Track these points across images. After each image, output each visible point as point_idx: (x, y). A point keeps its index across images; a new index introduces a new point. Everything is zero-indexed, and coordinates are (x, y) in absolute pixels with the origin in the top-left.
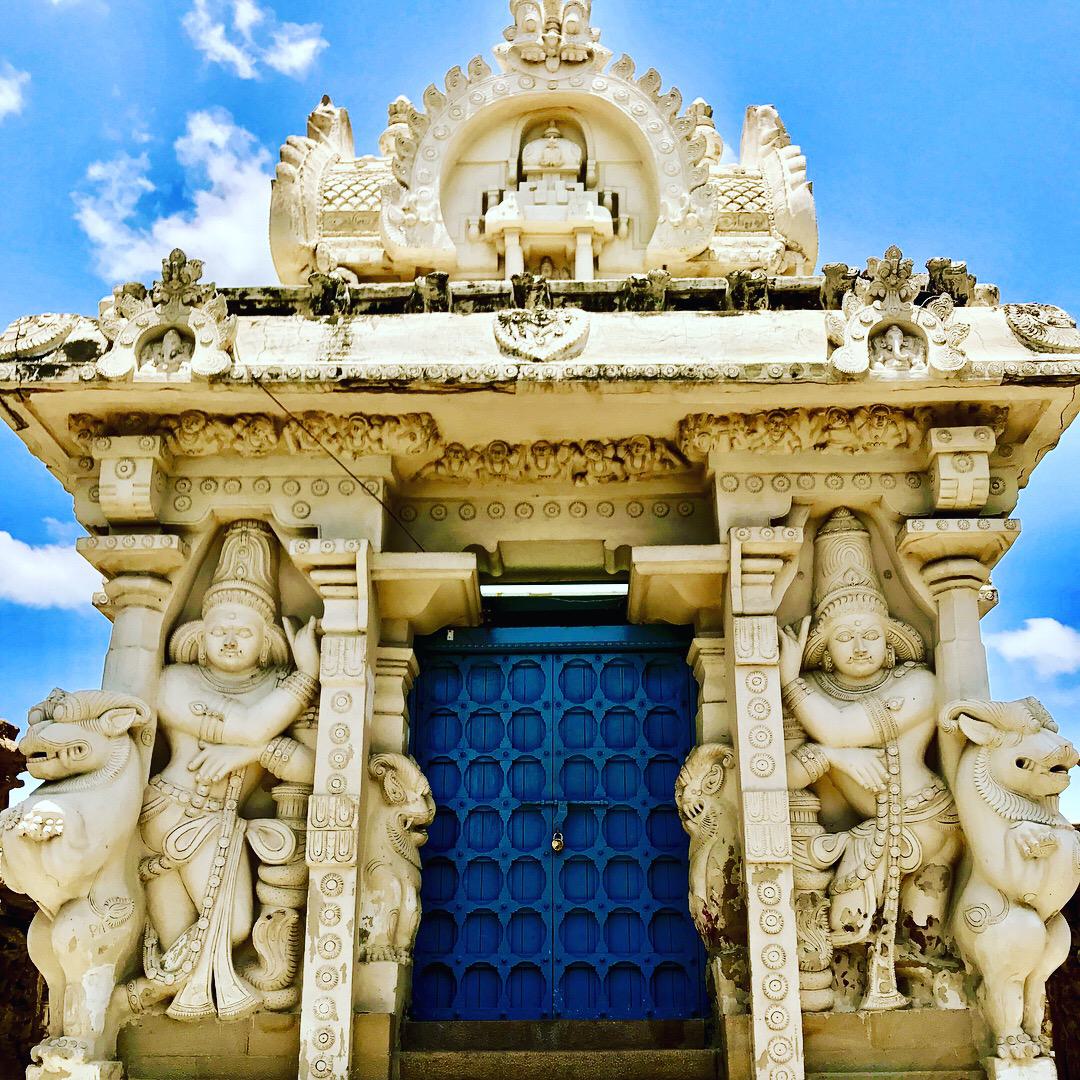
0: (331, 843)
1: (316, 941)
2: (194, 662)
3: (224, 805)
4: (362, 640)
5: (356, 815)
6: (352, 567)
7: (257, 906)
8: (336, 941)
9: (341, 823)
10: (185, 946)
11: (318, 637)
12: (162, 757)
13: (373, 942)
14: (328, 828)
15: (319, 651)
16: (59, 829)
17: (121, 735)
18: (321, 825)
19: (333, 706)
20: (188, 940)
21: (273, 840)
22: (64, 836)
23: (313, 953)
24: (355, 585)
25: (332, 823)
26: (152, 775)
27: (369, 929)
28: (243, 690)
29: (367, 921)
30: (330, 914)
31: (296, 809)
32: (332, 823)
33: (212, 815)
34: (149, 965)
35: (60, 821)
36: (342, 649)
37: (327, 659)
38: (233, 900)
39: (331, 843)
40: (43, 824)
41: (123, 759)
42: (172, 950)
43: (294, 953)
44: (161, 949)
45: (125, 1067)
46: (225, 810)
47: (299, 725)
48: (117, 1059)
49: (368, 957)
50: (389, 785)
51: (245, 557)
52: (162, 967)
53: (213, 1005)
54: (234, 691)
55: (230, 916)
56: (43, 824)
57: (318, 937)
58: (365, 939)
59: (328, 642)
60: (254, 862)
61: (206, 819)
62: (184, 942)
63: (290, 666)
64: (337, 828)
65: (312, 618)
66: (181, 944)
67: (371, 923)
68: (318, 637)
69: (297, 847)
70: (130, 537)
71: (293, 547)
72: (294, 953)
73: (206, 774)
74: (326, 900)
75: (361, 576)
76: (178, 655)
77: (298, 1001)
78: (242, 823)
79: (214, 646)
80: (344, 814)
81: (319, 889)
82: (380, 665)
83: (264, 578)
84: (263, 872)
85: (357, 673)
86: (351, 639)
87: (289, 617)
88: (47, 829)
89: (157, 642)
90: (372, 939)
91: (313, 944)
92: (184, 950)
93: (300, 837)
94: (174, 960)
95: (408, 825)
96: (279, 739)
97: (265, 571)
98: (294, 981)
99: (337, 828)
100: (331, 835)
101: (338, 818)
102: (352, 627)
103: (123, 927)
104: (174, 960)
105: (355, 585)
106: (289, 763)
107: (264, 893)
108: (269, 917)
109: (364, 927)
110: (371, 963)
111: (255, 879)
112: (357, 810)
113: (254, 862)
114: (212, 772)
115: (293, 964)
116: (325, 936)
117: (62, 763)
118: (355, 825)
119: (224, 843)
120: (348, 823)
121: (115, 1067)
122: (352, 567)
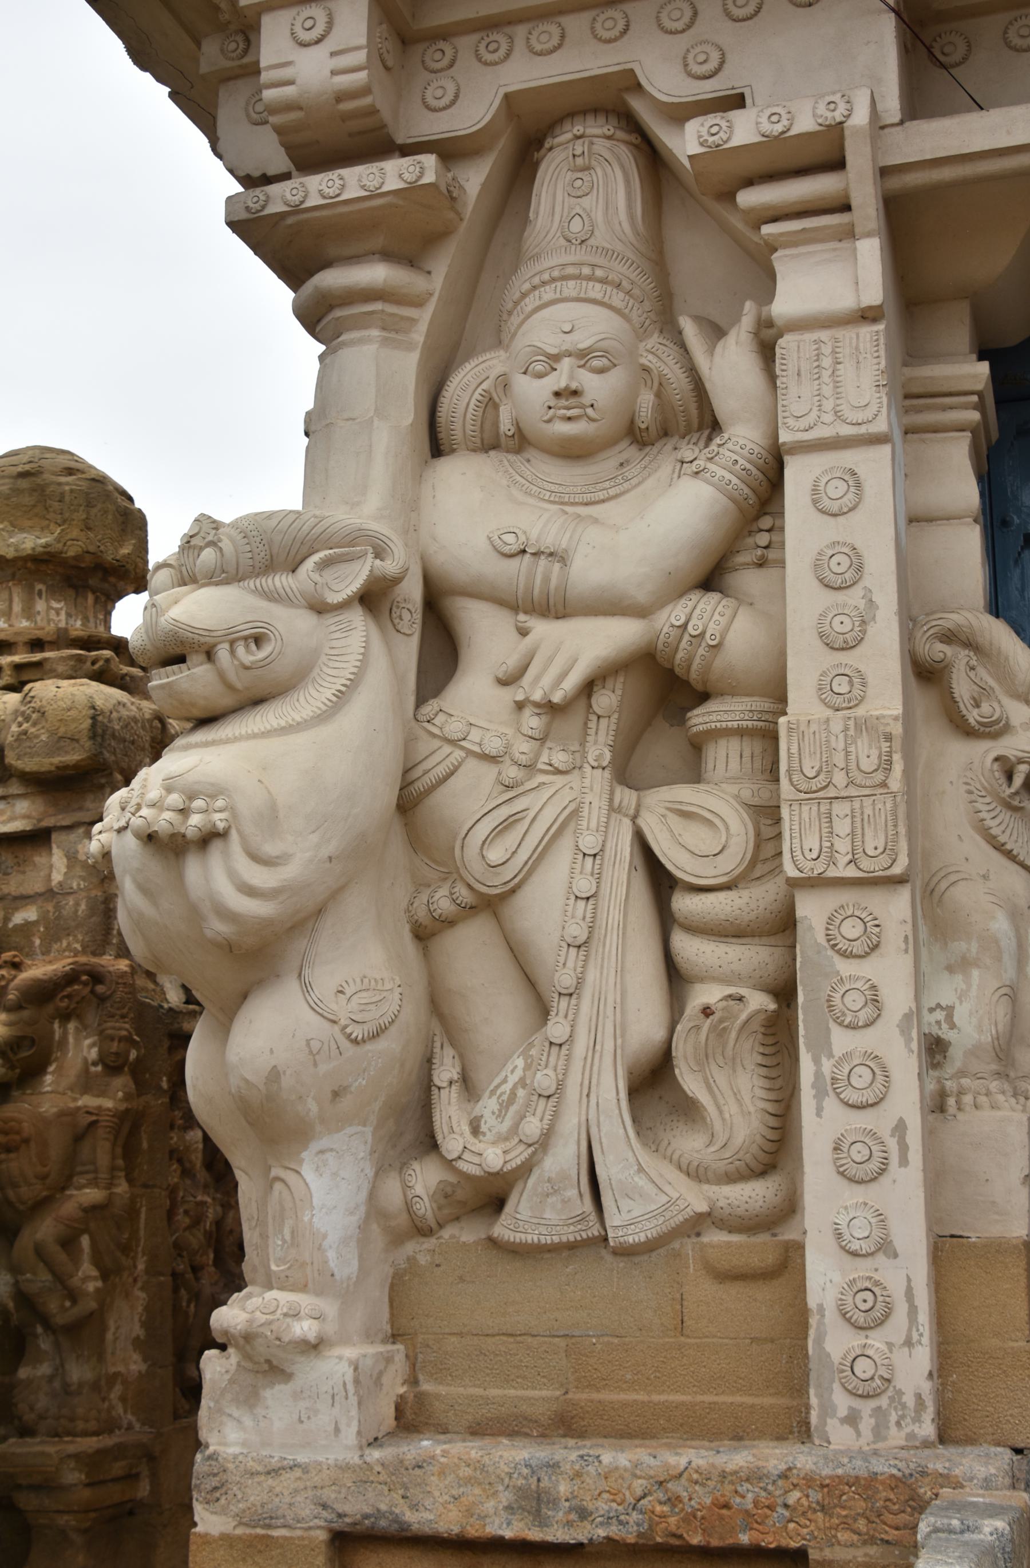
0: (843, 827)
1: (827, 1066)
2: (490, 443)
3: (584, 757)
4: (868, 333)
5: (897, 757)
6: (838, 164)
7: (676, 977)
8: (879, 1068)
9: (859, 779)
10: (522, 1082)
11: (767, 351)
12: (441, 651)
13: (958, 1064)
14: (831, 792)
15: (772, 378)
16: (219, 820)
17: (344, 606)
18: (814, 785)
19: (815, 502)
20: (527, 1067)
21: (701, 826)
22: (234, 835)
23: (820, 1094)
24: (847, 208)
25: (839, 779)
26: (421, 700)
27: (946, 1033)
28: (601, 495)
29: (939, 1015)
30: (855, 1001)
31: (747, 759)
32: (839, 779)
33: (559, 780)
34: (446, 1130)
35: (220, 803)
36: (827, 362)
37: (793, 391)
38: (621, 971)
39: (843, 827)
40: (184, 812)
41: (352, 661)
42: (493, 1092)
43: (772, 1096)
44: (468, 1085)
45: (412, 1360)
46: (588, 769)
47: (741, 558)
48: (395, 1337)
49: (951, 1101)
50: (962, 688)
51: (586, 196)
52: (476, 1131)
53: (593, 1217)
54: (587, 497)
55: (619, 1005)
56: (184, 812)
57: (831, 1055)
58: (938, 1057)
59: (793, 346)
60: (661, 881)
61: (546, 794)
62: (519, 1073)
63: (710, 425)
64: (853, 791)
65: (749, 306)
66: (513, 1079)
67: (950, 1018)
68: (767, 351)
69: (757, 847)
70: (334, 175)
71: (686, 143)
72: (772, 1096)
73: (538, 686)
74: (845, 967)
75: (860, 184)
76: (458, 435)
77: (790, 1207)
78: (626, 797)
79: (533, 394)
80: (867, 754)
81: (821, 939)
82: (915, 403)
83: (626, 226)
84: (683, 904)
85: (868, 414)
86: (847, 335)
87: (698, 319)
88: (195, 820)
89: (407, 412)
90: (957, 1056)
91: (818, 1075)
92: (521, 1093)
93: (767, 816)
94: (500, 1115)
95: (1018, 780)
96: (695, 596)
97: (631, 217)
98: (777, 1150)
99: (853, 791)
100: (840, 809)
101: (853, 766)
102: (845, 301)
103: (382, 1044)
104: (500, 1115)
105: (847, 208)
106: (722, 629)
107: (689, 948)
108: (707, 1011)
109: (935, 1031)
110: (960, 1116)
111: (666, 920)
112: (897, 744)
113: (661, 881)
114: (547, 681)
115: (773, 1122)
116: (847, 1056)
117: (222, 676)
118: (896, 782)
119: (589, 842)
120: (879, 777)
121: (389, 1360)
122: (838, 164)
